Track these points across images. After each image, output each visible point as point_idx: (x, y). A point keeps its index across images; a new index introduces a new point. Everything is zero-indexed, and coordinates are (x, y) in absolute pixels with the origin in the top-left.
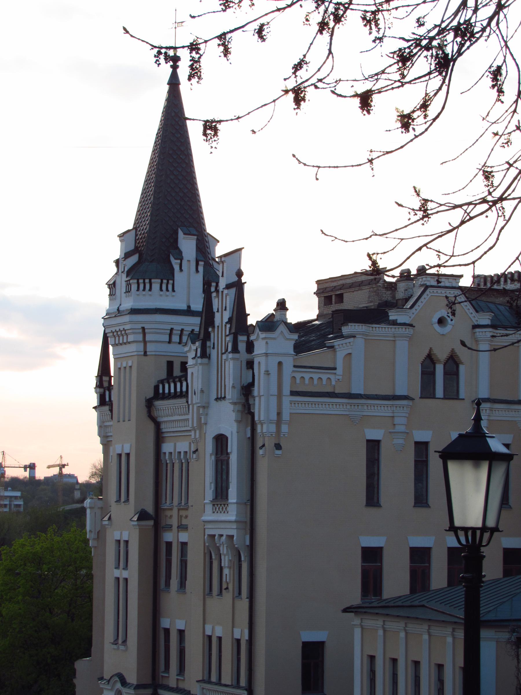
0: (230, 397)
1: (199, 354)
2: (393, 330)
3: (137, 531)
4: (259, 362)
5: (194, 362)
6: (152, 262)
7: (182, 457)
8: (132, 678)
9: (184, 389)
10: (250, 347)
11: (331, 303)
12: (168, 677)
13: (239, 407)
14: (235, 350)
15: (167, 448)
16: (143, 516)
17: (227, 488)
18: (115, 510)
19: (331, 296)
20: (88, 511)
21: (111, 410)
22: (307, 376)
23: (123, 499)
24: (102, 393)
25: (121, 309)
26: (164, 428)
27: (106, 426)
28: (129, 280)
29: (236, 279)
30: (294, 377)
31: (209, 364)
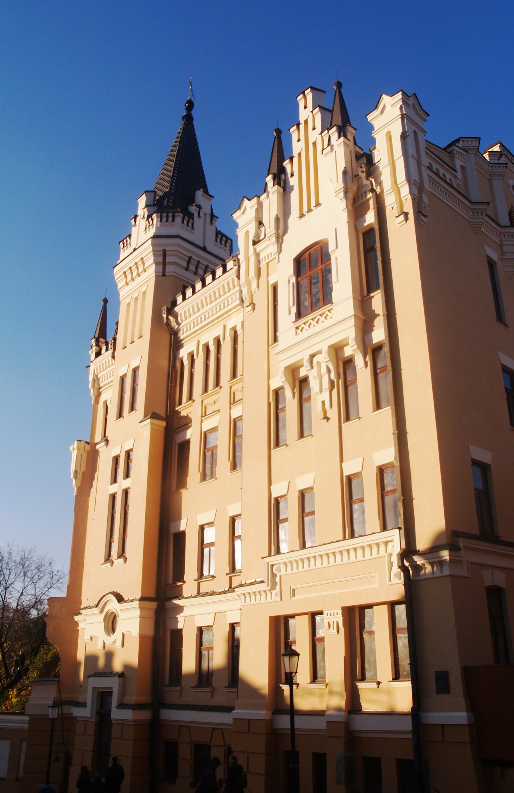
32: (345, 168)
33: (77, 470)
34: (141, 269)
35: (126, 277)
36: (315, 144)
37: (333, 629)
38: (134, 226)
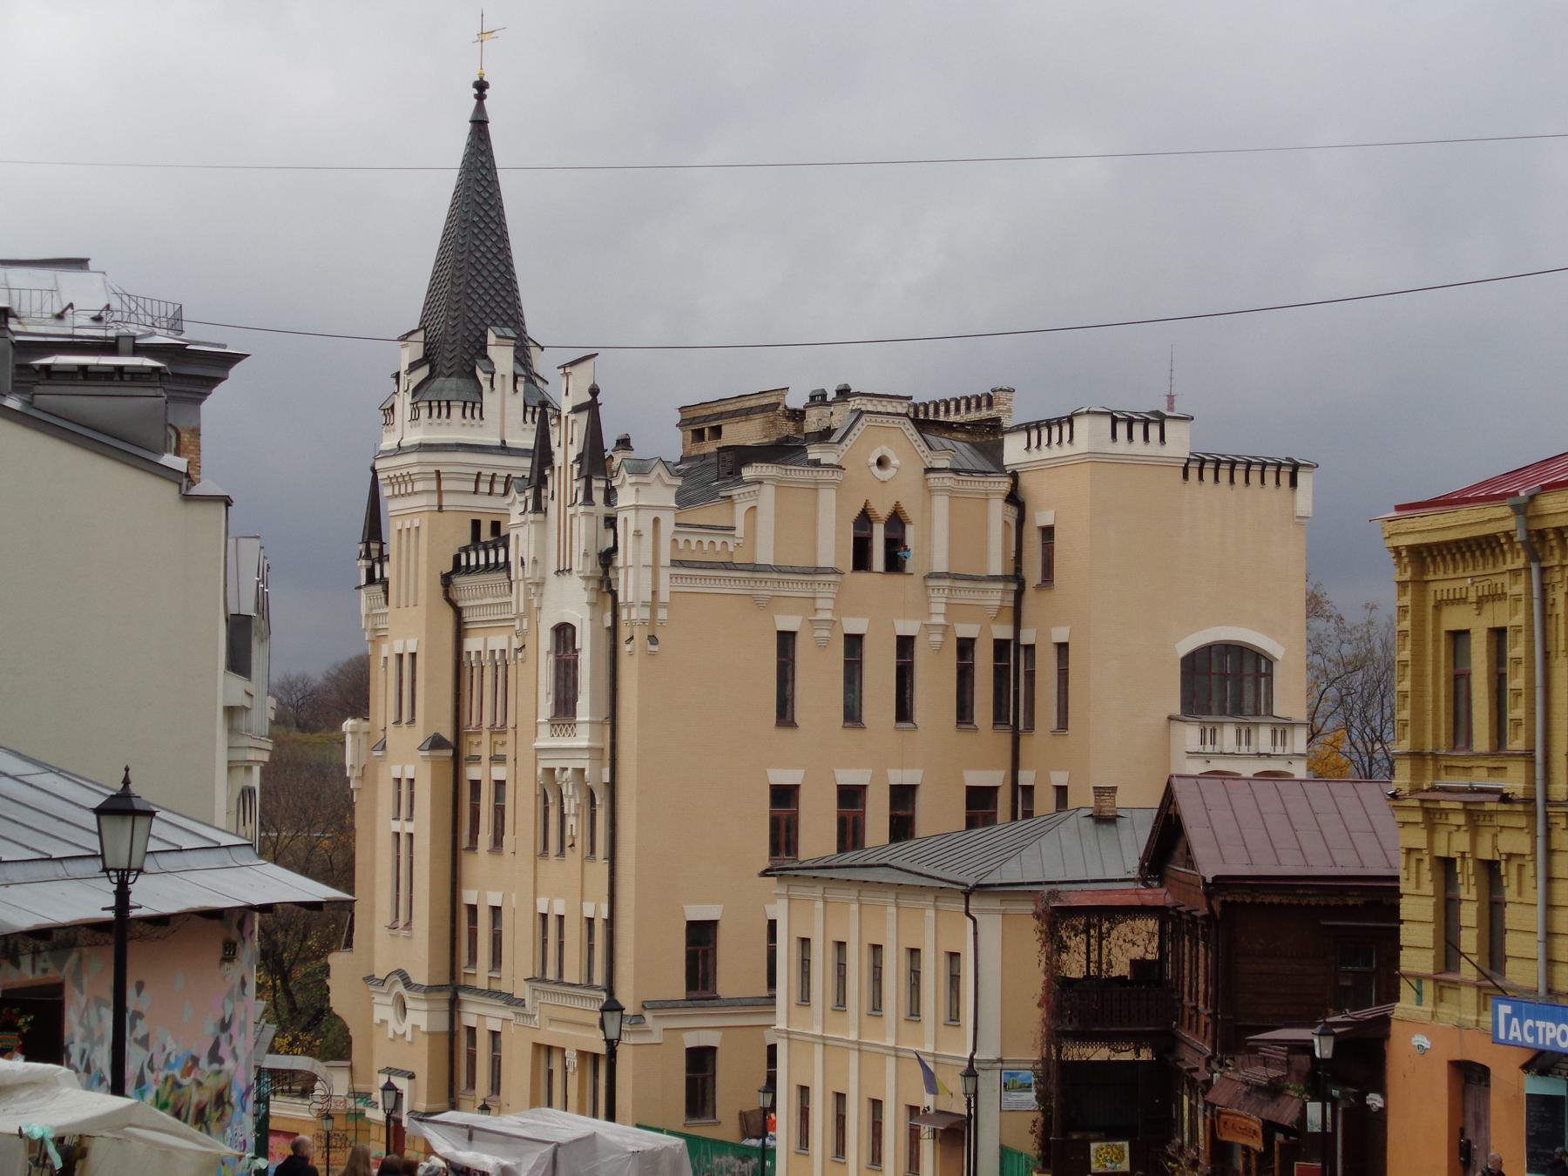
0: (581, 569)
1: (530, 507)
2: (815, 474)
3: (429, 765)
4: (626, 519)
5: (522, 518)
6: (449, 376)
7: (497, 656)
8: (421, 976)
9: (501, 559)
10: (610, 494)
11: (703, 440)
12: (475, 975)
13: (594, 584)
14: (588, 498)
15: (472, 644)
16: (436, 743)
17: (575, 699)
18: (396, 737)
19: (703, 429)
20: (349, 738)
21: (386, 592)
22: (694, 540)
23: (406, 717)
26: (468, 616)
27: (376, 615)
28: (417, 402)
29: (589, 398)
30: (675, 540)
31: (544, 522)
33: (356, 765)
36: (572, 466)
38: (395, 393)
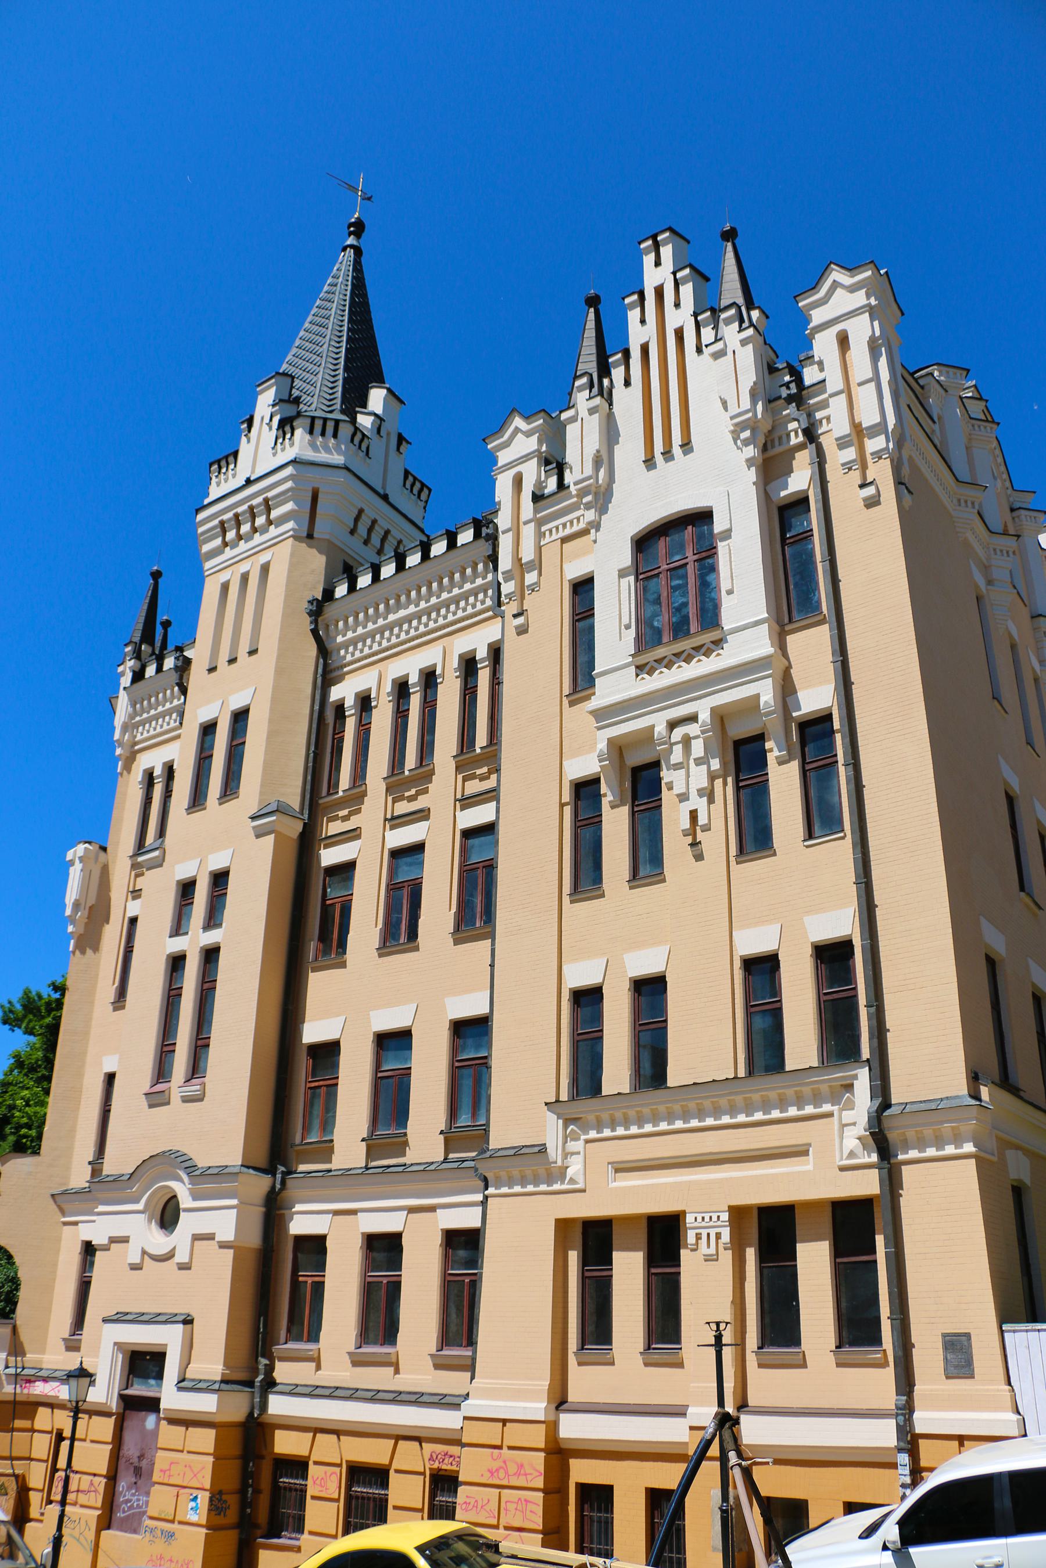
24: (137, 670)
25: (252, 479)
32: (755, 383)
34: (260, 521)
35: (224, 532)
37: (709, 1246)
